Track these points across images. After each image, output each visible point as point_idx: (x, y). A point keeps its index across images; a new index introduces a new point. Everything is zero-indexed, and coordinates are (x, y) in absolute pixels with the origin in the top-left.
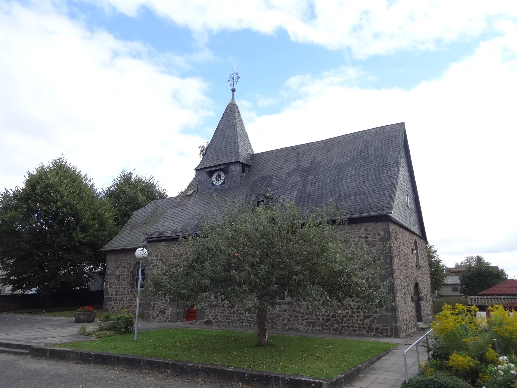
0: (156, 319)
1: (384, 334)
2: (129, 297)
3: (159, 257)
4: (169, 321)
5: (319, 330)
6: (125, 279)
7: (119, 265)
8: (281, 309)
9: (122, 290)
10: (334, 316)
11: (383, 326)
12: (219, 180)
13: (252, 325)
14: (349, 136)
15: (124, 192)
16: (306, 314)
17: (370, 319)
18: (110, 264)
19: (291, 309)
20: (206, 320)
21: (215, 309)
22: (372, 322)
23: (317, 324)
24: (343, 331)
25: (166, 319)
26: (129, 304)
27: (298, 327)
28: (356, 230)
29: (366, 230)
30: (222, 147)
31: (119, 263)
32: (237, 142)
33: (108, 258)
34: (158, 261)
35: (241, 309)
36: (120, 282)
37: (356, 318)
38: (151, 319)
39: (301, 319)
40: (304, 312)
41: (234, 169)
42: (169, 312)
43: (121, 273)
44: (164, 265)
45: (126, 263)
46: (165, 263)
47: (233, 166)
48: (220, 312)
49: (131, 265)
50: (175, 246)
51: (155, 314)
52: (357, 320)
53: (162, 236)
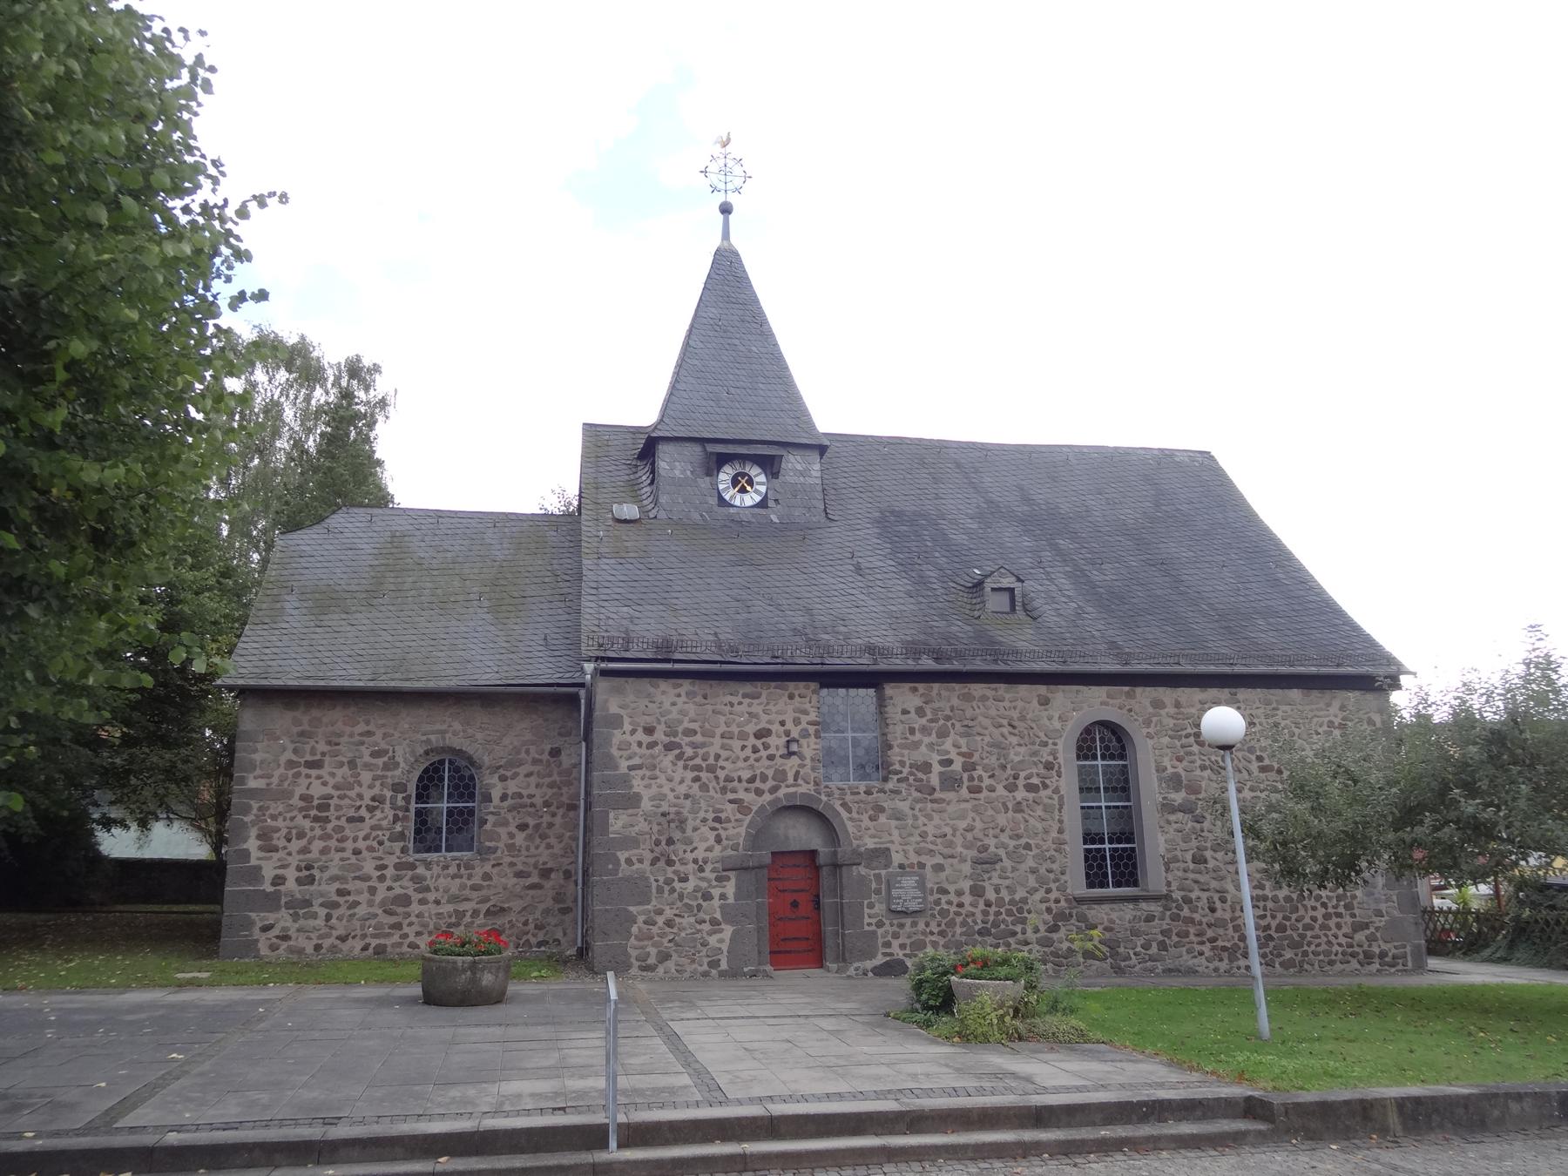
0: (661, 970)
1: (1400, 967)
2: (390, 889)
3: (659, 735)
4: (722, 974)
6: (363, 812)
7: (323, 754)
8: (1139, 913)
9: (342, 859)
10: (1281, 928)
11: (1395, 947)
12: (743, 490)
16: (1209, 925)
18: (259, 746)
19: (1168, 913)
20: (880, 960)
21: (914, 924)
22: (1371, 939)
23: (1240, 951)
24: (1306, 966)
25: (705, 967)
26: (393, 920)
27: (1190, 963)
28: (1322, 705)
29: (1342, 708)
31: (322, 747)
34: (657, 750)
35: (1009, 919)
36: (330, 826)
37: (1334, 930)
38: (634, 971)
39: (1195, 939)
40: (1204, 920)
41: (799, 467)
42: (721, 941)
43: (336, 787)
44: (685, 767)
45: (363, 748)
46: (692, 758)
47: (798, 458)
48: (932, 933)
49: (400, 759)
50: (735, 700)
51: (653, 951)
53: (677, 656)
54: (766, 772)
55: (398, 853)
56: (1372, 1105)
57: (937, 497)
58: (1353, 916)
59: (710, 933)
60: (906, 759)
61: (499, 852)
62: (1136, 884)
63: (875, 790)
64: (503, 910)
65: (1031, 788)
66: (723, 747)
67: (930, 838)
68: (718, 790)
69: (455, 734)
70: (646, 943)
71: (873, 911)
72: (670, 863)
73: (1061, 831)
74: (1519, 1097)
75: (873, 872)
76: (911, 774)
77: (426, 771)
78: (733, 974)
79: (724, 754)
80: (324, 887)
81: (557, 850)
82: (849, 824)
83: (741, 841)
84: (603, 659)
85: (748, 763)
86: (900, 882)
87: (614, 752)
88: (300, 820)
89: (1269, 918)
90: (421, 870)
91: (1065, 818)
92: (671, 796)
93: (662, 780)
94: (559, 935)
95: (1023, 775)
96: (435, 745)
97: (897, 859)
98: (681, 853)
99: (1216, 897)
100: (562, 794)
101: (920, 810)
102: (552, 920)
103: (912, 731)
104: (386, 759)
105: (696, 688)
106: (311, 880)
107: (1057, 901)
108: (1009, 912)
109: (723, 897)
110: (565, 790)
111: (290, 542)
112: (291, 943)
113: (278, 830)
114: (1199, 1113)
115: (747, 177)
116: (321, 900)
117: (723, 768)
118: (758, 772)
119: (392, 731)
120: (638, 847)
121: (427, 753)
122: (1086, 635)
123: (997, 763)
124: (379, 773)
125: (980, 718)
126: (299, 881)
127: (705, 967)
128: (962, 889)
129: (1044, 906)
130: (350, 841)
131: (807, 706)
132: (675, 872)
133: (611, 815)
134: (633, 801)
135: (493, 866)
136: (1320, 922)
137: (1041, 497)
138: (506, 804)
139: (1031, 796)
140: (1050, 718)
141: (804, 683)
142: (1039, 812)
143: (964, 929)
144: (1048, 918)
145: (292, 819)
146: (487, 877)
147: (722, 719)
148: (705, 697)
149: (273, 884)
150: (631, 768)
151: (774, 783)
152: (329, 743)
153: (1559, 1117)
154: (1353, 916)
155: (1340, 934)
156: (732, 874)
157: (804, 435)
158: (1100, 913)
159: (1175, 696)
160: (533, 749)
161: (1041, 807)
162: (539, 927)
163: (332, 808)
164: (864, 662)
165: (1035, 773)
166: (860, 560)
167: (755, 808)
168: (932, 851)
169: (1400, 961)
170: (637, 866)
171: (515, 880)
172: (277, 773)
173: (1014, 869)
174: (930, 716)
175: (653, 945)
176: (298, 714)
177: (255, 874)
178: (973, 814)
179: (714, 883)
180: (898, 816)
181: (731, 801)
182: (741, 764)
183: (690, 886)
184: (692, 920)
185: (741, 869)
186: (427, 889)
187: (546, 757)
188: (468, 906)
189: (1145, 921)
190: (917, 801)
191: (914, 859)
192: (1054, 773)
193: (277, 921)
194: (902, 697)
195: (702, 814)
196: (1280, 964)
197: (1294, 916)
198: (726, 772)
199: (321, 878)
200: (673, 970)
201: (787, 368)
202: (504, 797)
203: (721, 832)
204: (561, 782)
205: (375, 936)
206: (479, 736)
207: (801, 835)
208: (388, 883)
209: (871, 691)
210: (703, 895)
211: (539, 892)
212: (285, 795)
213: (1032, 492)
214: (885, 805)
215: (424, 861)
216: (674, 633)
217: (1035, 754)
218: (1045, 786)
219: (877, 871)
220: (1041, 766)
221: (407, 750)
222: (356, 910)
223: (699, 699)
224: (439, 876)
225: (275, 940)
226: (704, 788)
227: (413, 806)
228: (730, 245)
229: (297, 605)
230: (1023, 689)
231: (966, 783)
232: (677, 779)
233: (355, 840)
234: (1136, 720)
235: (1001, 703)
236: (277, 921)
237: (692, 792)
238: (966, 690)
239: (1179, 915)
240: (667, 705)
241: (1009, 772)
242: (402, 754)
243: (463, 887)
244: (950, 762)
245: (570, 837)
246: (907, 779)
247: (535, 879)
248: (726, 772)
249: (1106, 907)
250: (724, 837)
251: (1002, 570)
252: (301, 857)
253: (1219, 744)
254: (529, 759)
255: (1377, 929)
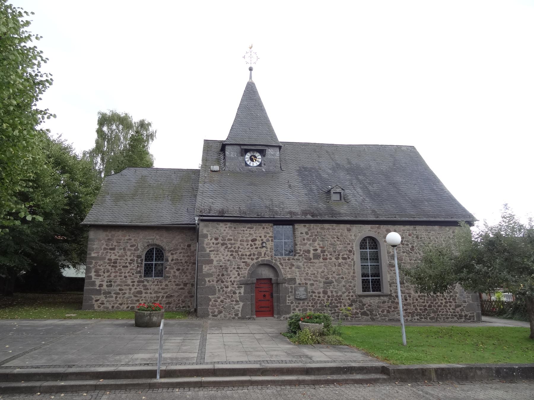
0: (219, 316)
2: (136, 289)
3: (220, 241)
4: (239, 318)
5: (418, 319)
6: (128, 264)
7: (115, 246)
8: (380, 301)
9: (121, 279)
10: (430, 306)
11: (470, 313)
13: (349, 318)
17: (460, 308)
18: (95, 243)
19: (390, 301)
21: (303, 303)
22: (462, 310)
23: (415, 314)
25: (234, 316)
26: (137, 299)
29: (453, 232)
30: (252, 126)
31: (115, 244)
33: (92, 234)
34: (219, 245)
35: (336, 302)
36: (117, 269)
37: (449, 307)
38: (210, 317)
43: (119, 256)
44: (228, 251)
45: (128, 244)
46: (230, 248)
47: (272, 150)
48: (309, 306)
49: (139, 248)
50: (245, 229)
51: (217, 310)
52: (449, 310)
53: (226, 215)
54: (255, 253)
55: (138, 277)
56: (426, 371)
57: (319, 162)
58: (455, 302)
59: (235, 305)
60: (302, 249)
61: (171, 277)
62: (380, 291)
63: (291, 259)
64: (171, 296)
65: (344, 259)
66: (241, 244)
67: (309, 275)
68: (239, 258)
69: (157, 239)
70: (214, 308)
71: (289, 299)
72: (222, 282)
73: (354, 273)
74: (480, 369)
75: (290, 286)
76: (303, 254)
77: (148, 251)
78: (243, 318)
79: (241, 247)
80: (115, 288)
81: (189, 277)
82: (282, 270)
83: (246, 275)
84: (201, 216)
85: (249, 250)
86: (299, 289)
87: (205, 246)
88: (108, 267)
89: (426, 303)
90: (145, 283)
91: (356, 270)
92: (223, 260)
93: (220, 255)
94: (190, 304)
95: (341, 254)
96: (150, 243)
97: (298, 281)
98: (226, 279)
99: (407, 295)
100: (191, 259)
101: (306, 266)
102: (188, 300)
103: (304, 239)
104: (135, 247)
105: (232, 225)
106: (111, 286)
107: (352, 296)
108: (336, 300)
109: (240, 293)
110: (192, 258)
111: (109, 179)
112: (105, 305)
113: (101, 270)
114: (365, 371)
115: (258, 58)
116: (114, 292)
117: (240, 251)
118: (252, 253)
119: (137, 239)
120: (212, 277)
121: (148, 246)
122: (365, 208)
123: (333, 250)
124: (133, 252)
125: (327, 235)
126: (107, 286)
127: (234, 316)
128: (320, 292)
129: (347, 298)
130: (124, 273)
131: (269, 231)
132: (224, 285)
133: (204, 266)
134: (211, 262)
135: (169, 282)
136: (444, 304)
137: (354, 162)
138: (173, 262)
139: (344, 261)
140: (351, 235)
141: (268, 224)
142: (347, 266)
143: (320, 305)
144: (349, 301)
145: (105, 266)
146: (167, 285)
147: (241, 235)
148: (235, 228)
149: (99, 287)
150: (210, 251)
151: (257, 256)
152: (117, 242)
153: (495, 376)
154: (455, 302)
155: (451, 308)
156: (243, 286)
157: (274, 142)
158: (366, 300)
159: (394, 228)
160: (182, 245)
161: (347, 265)
162: (183, 302)
163: (118, 263)
164: (288, 217)
165: (345, 254)
166: (291, 183)
167: (251, 265)
168: (310, 279)
169: (472, 318)
170: (212, 283)
171: (175, 287)
172: (101, 252)
173: (338, 285)
174: (310, 235)
175: (217, 308)
176: (107, 233)
177: (93, 283)
178: (324, 267)
179: (237, 289)
180: (298, 267)
181: (243, 262)
182: (246, 250)
183: (229, 289)
184: (229, 300)
185: (246, 284)
186: (148, 289)
187: (186, 247)
188: (161, 295)
189: (382, 303)
190: (305, 262)
191: (304, 281)
192: (352, 254)
193: (100, 298)
194: (301, 228)
195: (233, 266)
196: (429, 318)
197: (435, 302)
198: (241, 253)
199: (114, 285)
200: (223, 317)
201: (269, 121)
202: (172, 260)
203: (240, 272)
204: (191, 255)
205: (131, 304)
206: (165, 240)
207: (266, 273)
208: (135, 287)
209: (291, 226)
210: (233, 292)
211: (183, 290)
212: (103, 259)
213: (351, 160)
214: (294, 264)
215: (147, 280)
216: (226, 207)
217: (346, 247)
218: (349, 258)
219: (291, 286)
220: (347, 251)
221: (142, 245)
222: (125, 295)
223: (233, 229)
224: (151, 285)
225: (99, 304)
226: (234, 258)
227: (144, 262)
228: (252, 81)
229: (110, 198)
230: (342, 226)
231: (322, 257)
232: (225, 254)
233: (125, 273)
234: (380, 236)
235: (334, 231)
236: (100, 298)
237: (230, 259)
238: (322, 226)
239: (394, 301)
240: (222, 231)
241: (337, 253)
242: (140, 246)
243: (159, 288)
244: (316, 250)
245: (193, 273)
246: (302, 255)
247: (182, 286)
248: (241, 253)
249: (369, 298)
250: (240, 274)
251: (337, 186)
252: (108, 278)
253: (392, 245)
254: (181, 248)
255: (464, 307)
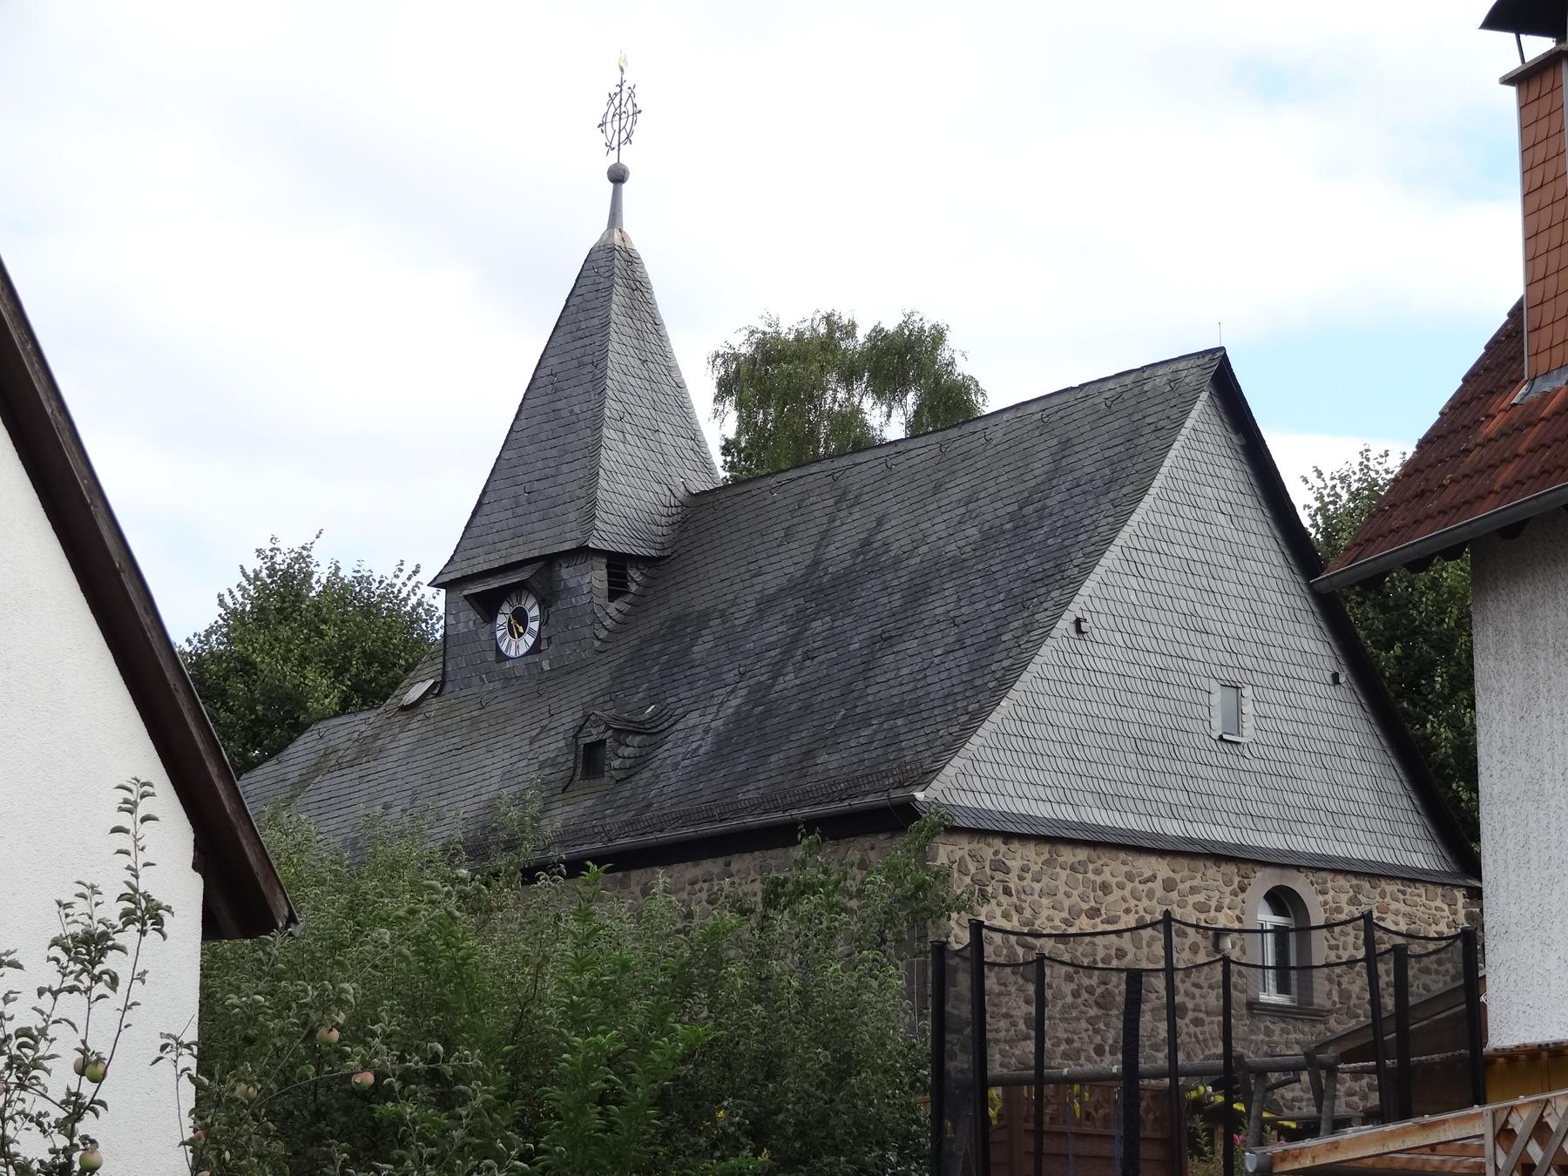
14: (1033, 408)
15: (246, 667)
32: (596, 446)
